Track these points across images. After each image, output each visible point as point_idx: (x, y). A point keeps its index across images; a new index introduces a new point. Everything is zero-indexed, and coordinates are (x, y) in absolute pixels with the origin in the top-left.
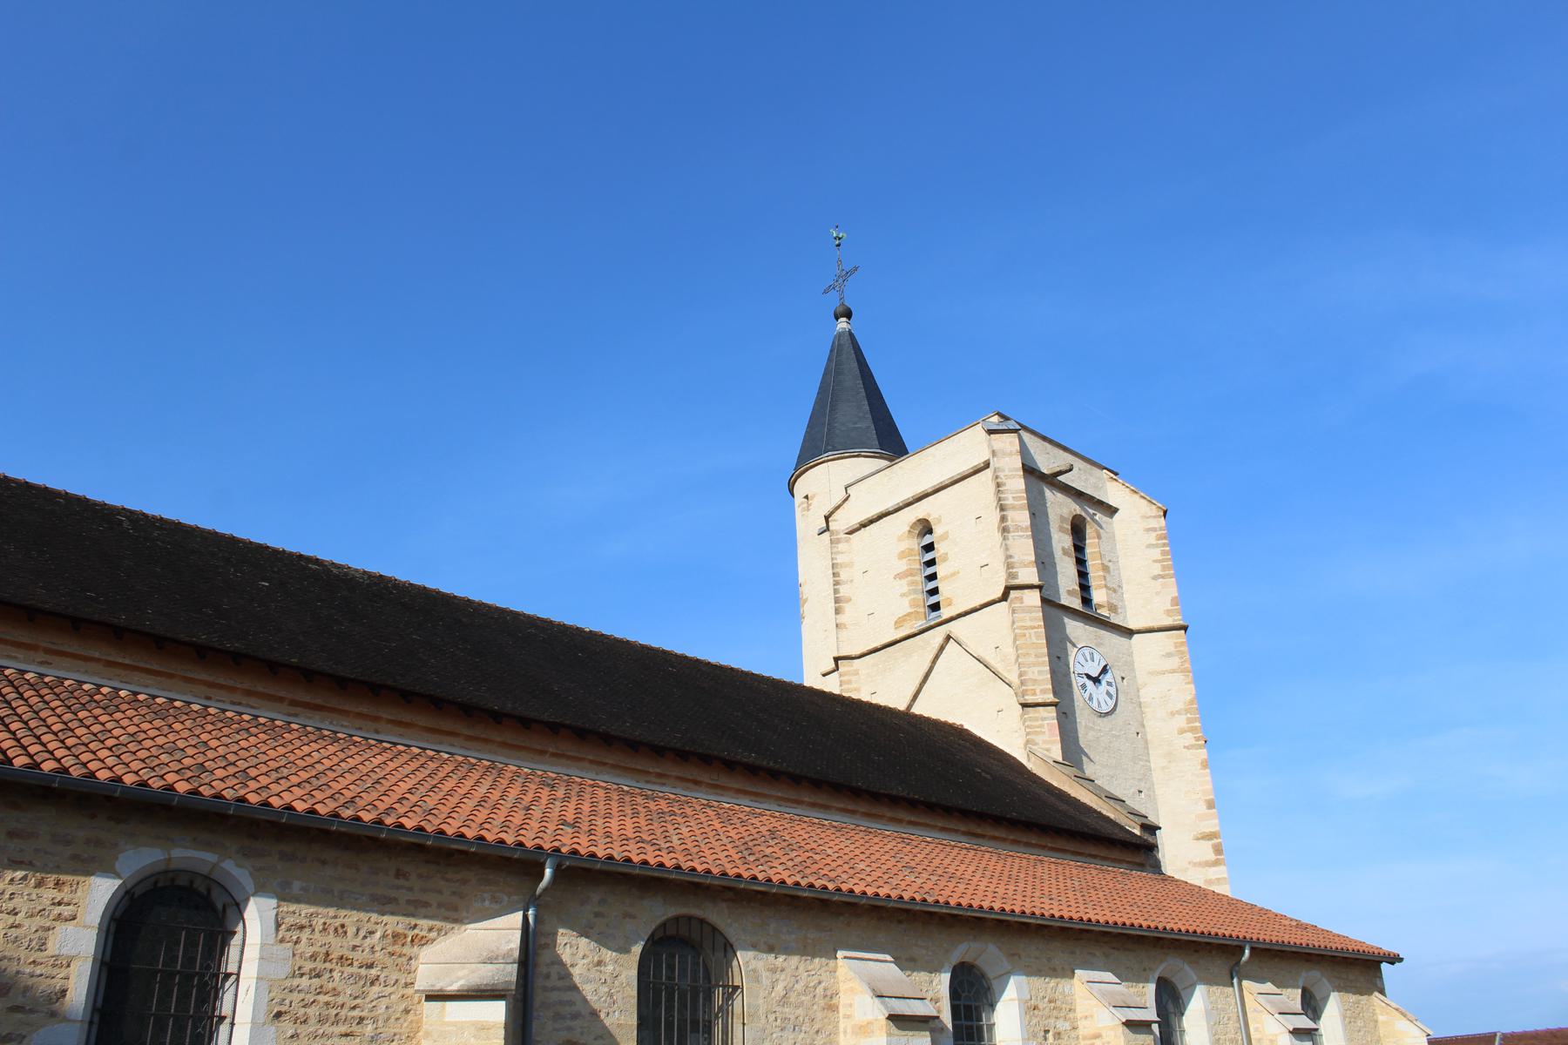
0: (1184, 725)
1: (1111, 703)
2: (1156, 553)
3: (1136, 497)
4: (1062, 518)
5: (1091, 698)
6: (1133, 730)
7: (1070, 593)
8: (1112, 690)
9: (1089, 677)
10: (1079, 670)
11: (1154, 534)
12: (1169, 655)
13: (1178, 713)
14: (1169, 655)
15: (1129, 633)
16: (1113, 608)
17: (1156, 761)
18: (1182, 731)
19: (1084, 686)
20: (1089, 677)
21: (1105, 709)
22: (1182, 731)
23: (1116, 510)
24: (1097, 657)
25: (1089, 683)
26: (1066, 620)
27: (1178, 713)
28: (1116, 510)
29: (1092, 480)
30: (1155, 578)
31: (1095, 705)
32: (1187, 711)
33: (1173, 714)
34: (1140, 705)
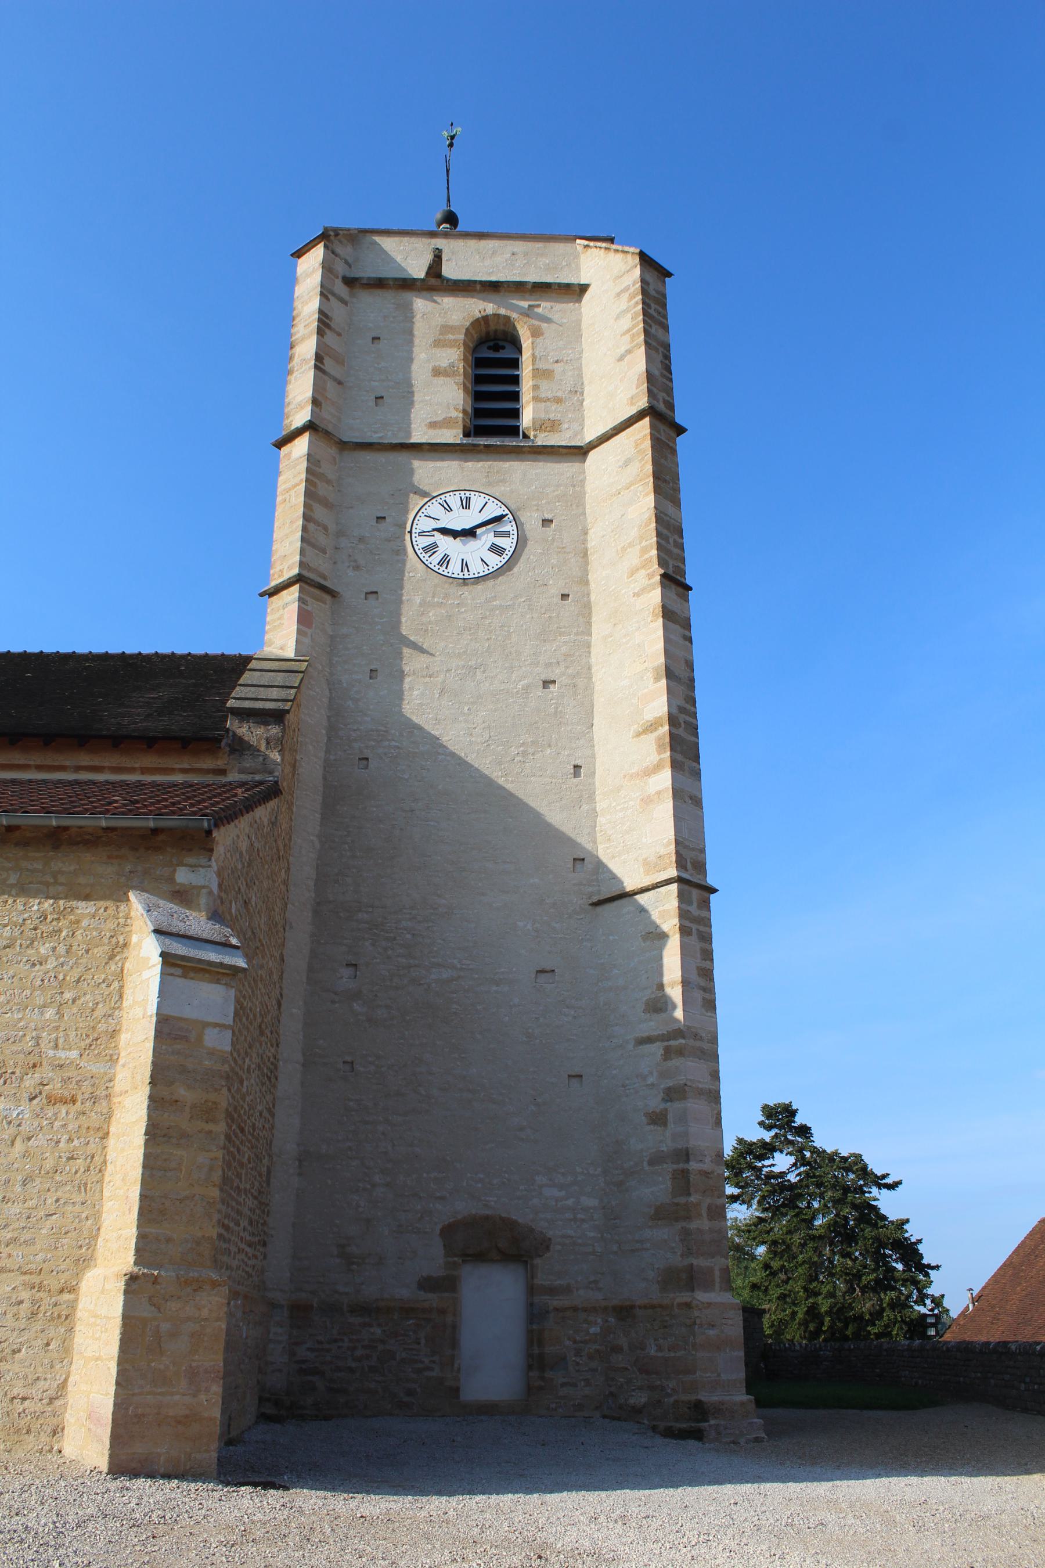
0: (636, 561)
1: (495, 561)
2: (626, 322)
3: (611, 254)
4: (446, 329)
5: (445, 560)
6: (555, 591)
7: (433, 425)
8: (508, 544)
9: (444, 531)
10: (424, 524)
11: (626, 296)
12: (627, 463)
13: (631, 545)
14: (627, 463)
15: (581, 452)
16: (553, 426)
17: (600, 627)
18: (633, 572)
19: (432, 548)
20: (444, 531)
21: (477, 569)
22: (633, 572)
23: (583, 288)
24: (477, 501)
25: (446, 543)
26: (416, 464)
27: (631, 545)
28: (583, 288)
29: (543, 261)
30: (621, 359)
31: (454, 569)
32: (641, 538)
33: (624, 549)
34: (585, 554)
